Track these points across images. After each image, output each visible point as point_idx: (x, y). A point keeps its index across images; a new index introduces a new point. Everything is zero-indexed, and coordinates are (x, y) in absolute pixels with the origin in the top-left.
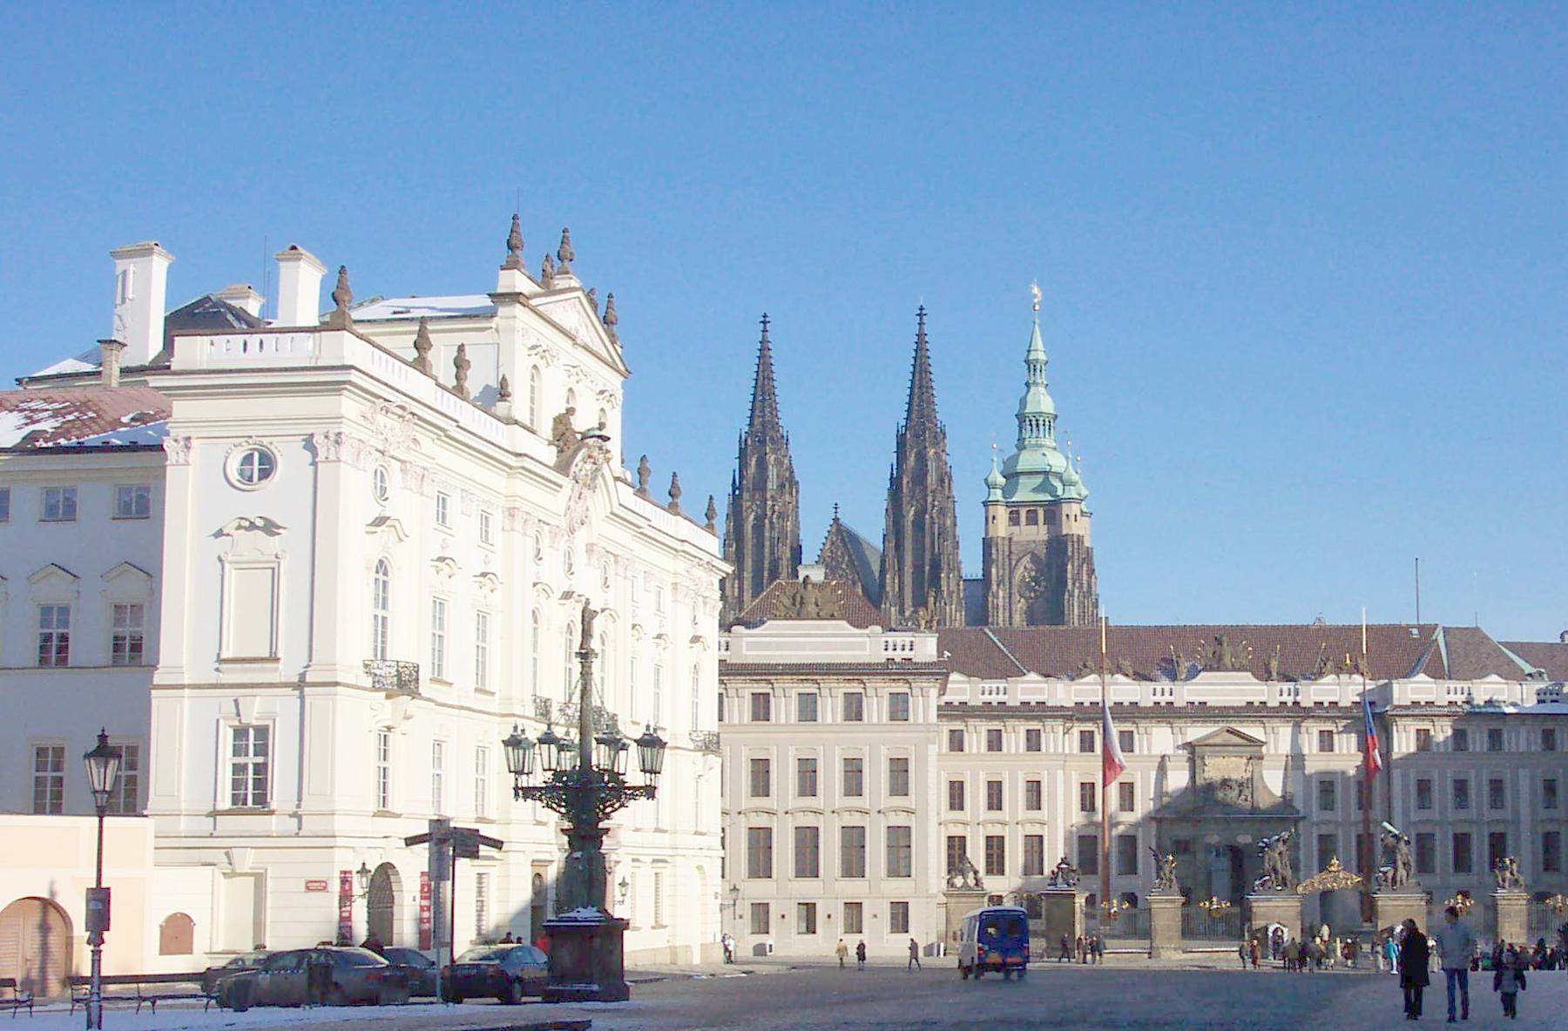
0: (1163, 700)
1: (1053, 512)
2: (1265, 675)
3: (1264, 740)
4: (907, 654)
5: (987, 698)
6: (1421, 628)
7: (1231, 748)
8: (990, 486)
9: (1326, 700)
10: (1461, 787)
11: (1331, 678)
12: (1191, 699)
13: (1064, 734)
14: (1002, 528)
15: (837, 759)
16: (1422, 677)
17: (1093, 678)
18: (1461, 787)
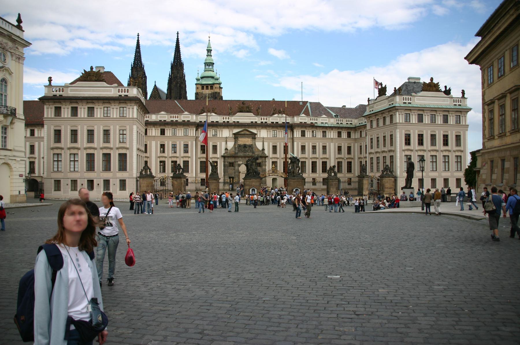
0: (226, 120)
1: (213, 86)
2: (257, 114)
3: (256, 133)
4: (126, 94)
5: (172, 119)
6: (303, 102)
7: (246, 135)
8: (198, 80)
9: (275, 121)
10: (314, 147)
11: (276, 115)
12: (234, 121)
13: (196, 131)
14: (200, 90)
15: (101, 130)
16: (303, 115)
17: (205, 114)
18: (314, 147)
